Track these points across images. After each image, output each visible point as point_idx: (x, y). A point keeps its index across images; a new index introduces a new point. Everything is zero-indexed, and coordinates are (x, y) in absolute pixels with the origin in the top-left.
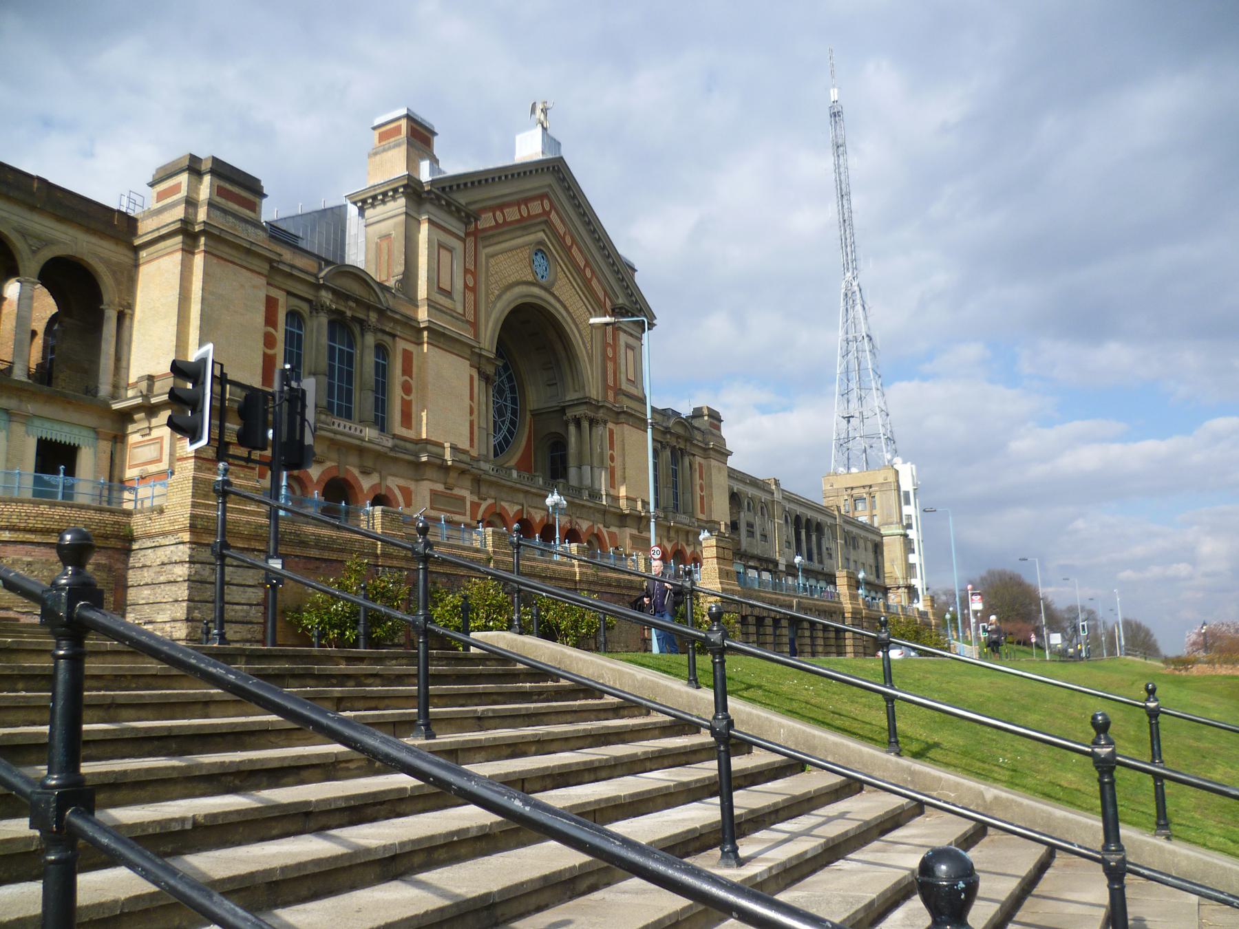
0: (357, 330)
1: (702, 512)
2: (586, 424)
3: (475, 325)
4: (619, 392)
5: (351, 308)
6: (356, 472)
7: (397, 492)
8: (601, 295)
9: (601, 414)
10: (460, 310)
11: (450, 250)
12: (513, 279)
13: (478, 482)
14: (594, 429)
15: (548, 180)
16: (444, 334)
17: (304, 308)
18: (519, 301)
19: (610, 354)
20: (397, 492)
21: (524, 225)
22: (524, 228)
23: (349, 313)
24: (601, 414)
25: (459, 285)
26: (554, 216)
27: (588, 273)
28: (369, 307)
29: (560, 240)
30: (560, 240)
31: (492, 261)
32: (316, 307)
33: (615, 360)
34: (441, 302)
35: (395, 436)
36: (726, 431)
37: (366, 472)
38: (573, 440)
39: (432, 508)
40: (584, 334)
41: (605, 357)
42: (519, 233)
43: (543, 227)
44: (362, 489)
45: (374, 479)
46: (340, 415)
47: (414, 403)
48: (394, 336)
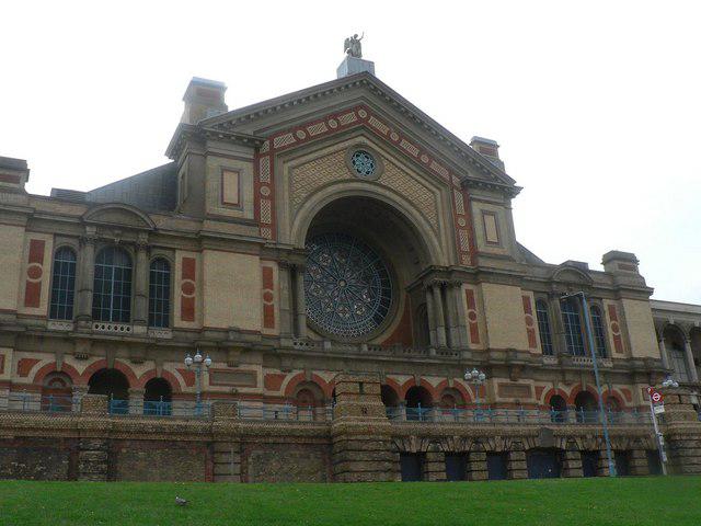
0: (131, 250)
1: (619, 350)
2: (437, 291)
3: (274, 226)
4: (475, 253)
5: (117, 235)
6: (127, 363)
7: (178, 376)
8: (445, 174)
9: (455, 278)
10: (250, 215)
11: (238, 172)
12: (325, 180)
13: (272, 355)
14: (448, 294)
15: (361, 93)
16: (223, 239)
17: (74, 243)
18: (341, 196)
19: (462, 222)
20: (178, 376)
21: (334, 136)
22: (335, 137)
23: (117, 240)
24: (455, 278)
25: (248, 195)
27: (425, 159)
28: (137, 231)
29: (384, 140)
30: (384, 140)
32: (83, 241)
33: (470, 228)
34: (225, 214)
35: (174, 329)
36: (643, 270)
37: (138, 362)
38: (430, 306)
39: (211, 384)
40: (425, 211)
41: (455, 227)
42: (332, 142)
43: (363, 132)
44: (134, 376)
45: (149, 366)
46: (116, 319)
47: (196, 299)
48: (174, 250)
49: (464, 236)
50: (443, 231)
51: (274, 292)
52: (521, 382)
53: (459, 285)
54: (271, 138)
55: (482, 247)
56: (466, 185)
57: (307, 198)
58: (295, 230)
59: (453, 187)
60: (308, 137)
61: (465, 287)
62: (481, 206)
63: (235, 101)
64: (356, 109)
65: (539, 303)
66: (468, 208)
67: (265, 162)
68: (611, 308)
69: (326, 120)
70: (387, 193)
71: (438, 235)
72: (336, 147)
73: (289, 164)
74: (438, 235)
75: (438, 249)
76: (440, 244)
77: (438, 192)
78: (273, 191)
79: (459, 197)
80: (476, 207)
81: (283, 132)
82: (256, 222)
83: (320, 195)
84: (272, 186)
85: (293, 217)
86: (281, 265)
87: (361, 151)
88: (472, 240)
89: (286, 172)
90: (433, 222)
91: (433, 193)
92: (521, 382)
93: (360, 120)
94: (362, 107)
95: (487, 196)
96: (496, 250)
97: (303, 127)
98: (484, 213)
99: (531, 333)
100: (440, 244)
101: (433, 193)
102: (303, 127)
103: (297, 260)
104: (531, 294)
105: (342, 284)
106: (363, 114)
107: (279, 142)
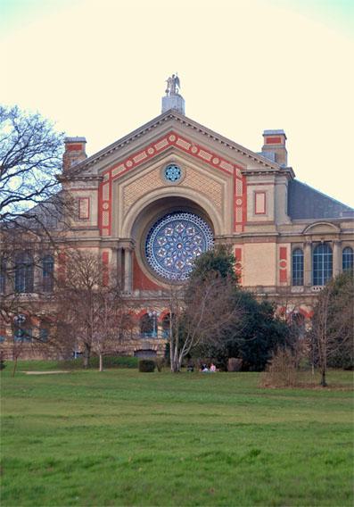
4: (245, 223)
21: (152, 159)
25: (94, 211)
26: (180, 142)
31: (127, 188)
50: (225, 209)
54: (110, 171)
55: (250, 217)
56: (246, 174)
57: (132, 205)
58: (124, 228)
59: (235, 177)
60: (134, 164)
62: (254, 188)
63: (91, 150)
64: (167, 136)
65: (294, 251)
66: (245, 191)
67: (106, 188)
69: (146, 149)
70: (187, 191)
72: (154, 166)
73: (123, 185)
75: (221, 224)
76: (223, 218)
77: (225, 182)
78: (110, 205)
79: (239, 184)
80: (250, 190)
81: (118, 164)
82: (99, 227)
83: (142, 201)
84: (109, 202)
85: (124, 218)
87: (170, 165)
88: (245, 214)
89: (121, 189)
93: (171, 143)
94: (172, 133)
95: (261, 179)
96: (264, 219)
97: (130, 158)
98: (256, 193)
99: (283, 273)
100: (223, 218)
102: (130, 158)
103: (125, 245)
105: (180, 246)
106: (172, 138)
107: (115, 172)
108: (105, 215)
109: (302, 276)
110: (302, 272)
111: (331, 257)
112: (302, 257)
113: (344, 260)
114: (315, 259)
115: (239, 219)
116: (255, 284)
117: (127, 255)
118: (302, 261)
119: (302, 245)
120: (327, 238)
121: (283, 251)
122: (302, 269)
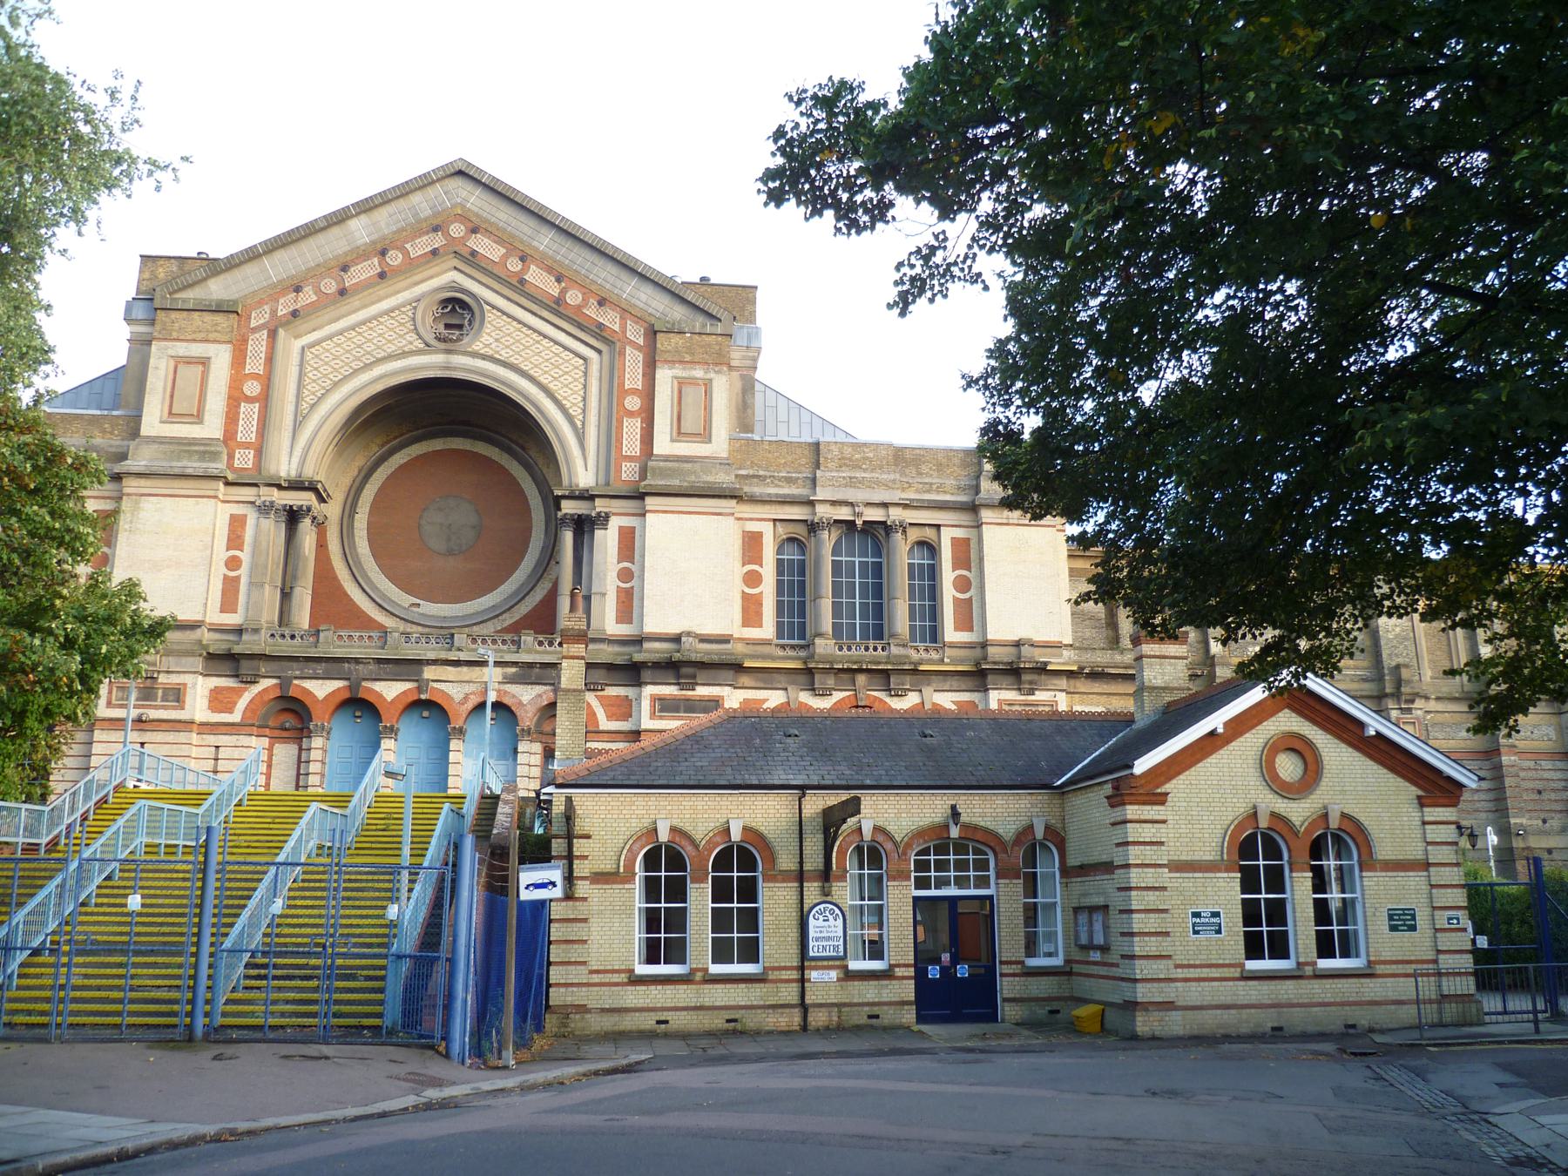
9: (601, 506)
49: (632, 430)
51: (245, 556)
52: (702, 691)
53: (603, 520)
61: (615, 523)
67: (257, 346)
68: (961, 546)
71: (581, 438)
74: (581, 438)
80: (665, 377)
86: (265, 509)
90: (575, 412)
91: (585, 359)
92: (702, 691)
98: (682, 384)
101: (585, 359)
104: (767, 530)
106: (457, 230)
108: (249, 414)
109: (802, 614)
110: (802, 604)
111: (878, 569)
112: (802, 564)
113: (911, 577)
114: (836, 566)
115: (631, 442)
116: (674, 629)
117: (306, 525)
118: (802, 573)
119: (801, 531)
120: (874, 515)
121: (752, 544)
122: (802, 593)
